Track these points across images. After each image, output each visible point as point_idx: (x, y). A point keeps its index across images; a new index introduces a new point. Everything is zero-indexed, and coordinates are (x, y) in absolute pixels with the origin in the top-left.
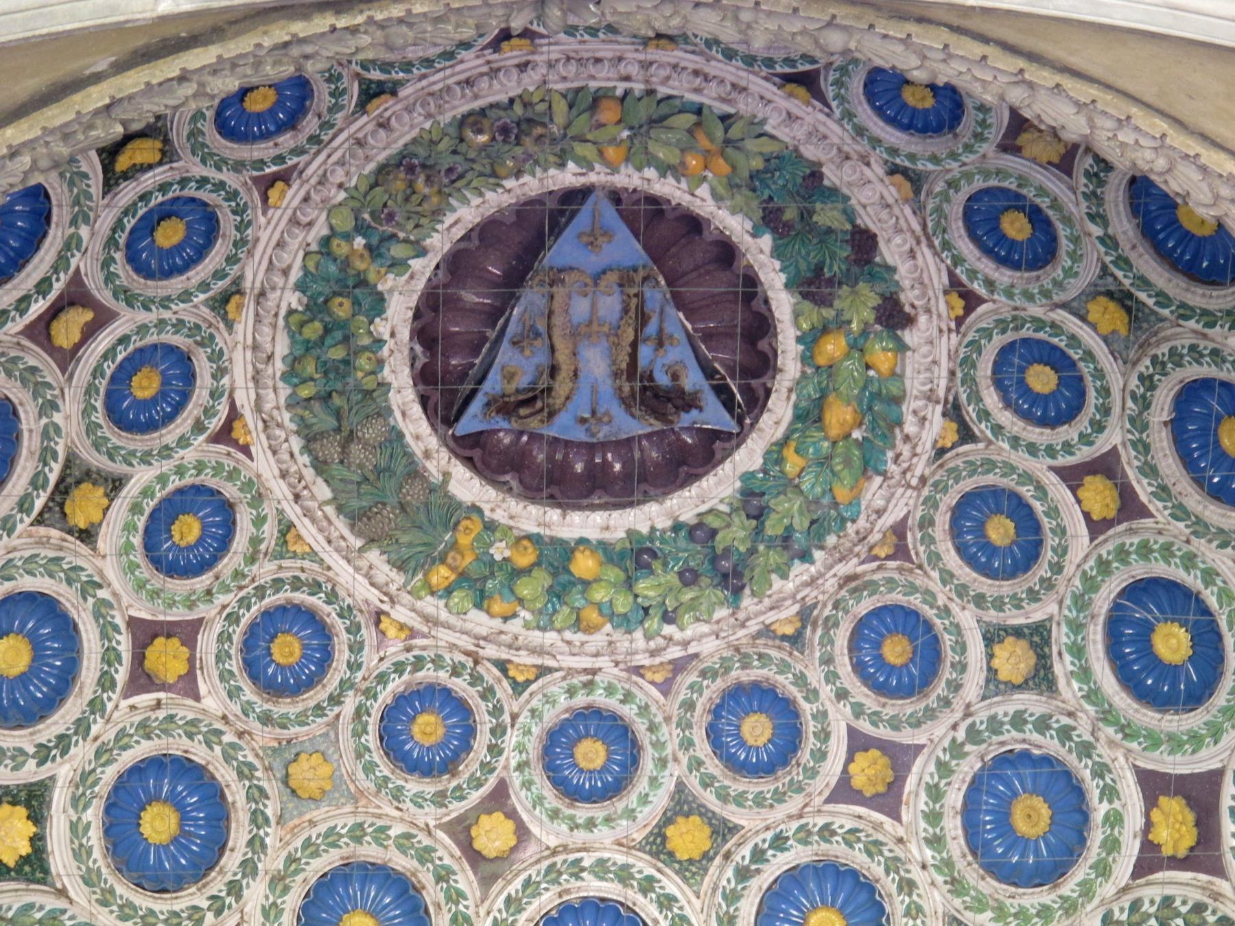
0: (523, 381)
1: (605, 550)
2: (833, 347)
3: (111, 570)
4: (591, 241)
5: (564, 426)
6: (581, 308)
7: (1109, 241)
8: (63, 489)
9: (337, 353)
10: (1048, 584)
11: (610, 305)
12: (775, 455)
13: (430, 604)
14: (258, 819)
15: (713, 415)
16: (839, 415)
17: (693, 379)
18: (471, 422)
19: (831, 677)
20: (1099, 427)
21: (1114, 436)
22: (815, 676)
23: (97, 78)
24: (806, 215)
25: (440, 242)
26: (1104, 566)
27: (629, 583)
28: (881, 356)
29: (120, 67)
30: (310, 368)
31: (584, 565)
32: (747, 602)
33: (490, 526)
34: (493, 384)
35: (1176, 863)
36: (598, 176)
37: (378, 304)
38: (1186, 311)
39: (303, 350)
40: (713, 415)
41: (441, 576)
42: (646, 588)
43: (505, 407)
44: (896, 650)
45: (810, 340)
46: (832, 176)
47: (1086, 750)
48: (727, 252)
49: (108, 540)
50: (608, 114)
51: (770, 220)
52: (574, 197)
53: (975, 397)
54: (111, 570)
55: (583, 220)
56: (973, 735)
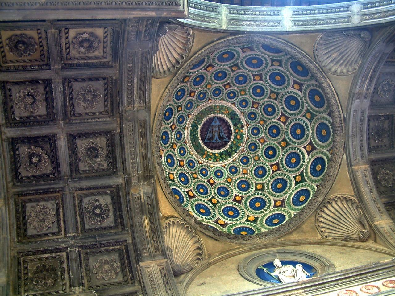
0: (210, 137)
1: (218, 153)
2: (237, 131)
3: (177, 154)
4: (216, 122)
5: (214, 141)
6: (215, 129)
7: (262, 114)
8: (172, 145)
9: (195, 133)
10: (258, 150)
11: (217, 129)
12: (232, 142)
13: (204, 159)
14: (191, 179)
15: (227, 140)
16: (238, 137)
17: (224, 136)
18: (206, 141)
19: (239, 164)
20: (261, 134)
21: (263, 135)
22: (238, 164)
23: (215, 41)
24: (234, 117)
25: (203, 122)
26: (264, 147)
27: (221, 157)
28: (241, 131)
29: (217, 40)
30: (192, 134)
31: (217, 155)
32: (231, 157)
33: (208, 152)
34: (207, 137)
35: (276, 171)
36: (217, 115)
37: (197, 129)
38: (269, 119)
39: (191, 132)
40: (227, 140)
41: (204, 156)
42: (222, 156)
43: (209, 139)
44: (245, 161)
45: (235, 130)
46: (237, 113)
47: (265, 164)
48: (227, 123)
49: (176, 150)
50: (218, 107)
51: (231, 119)
52: (214, 117)
53: (250, 134)
54: (177, 154)
55: (215, 120)
56: (254, 166)
